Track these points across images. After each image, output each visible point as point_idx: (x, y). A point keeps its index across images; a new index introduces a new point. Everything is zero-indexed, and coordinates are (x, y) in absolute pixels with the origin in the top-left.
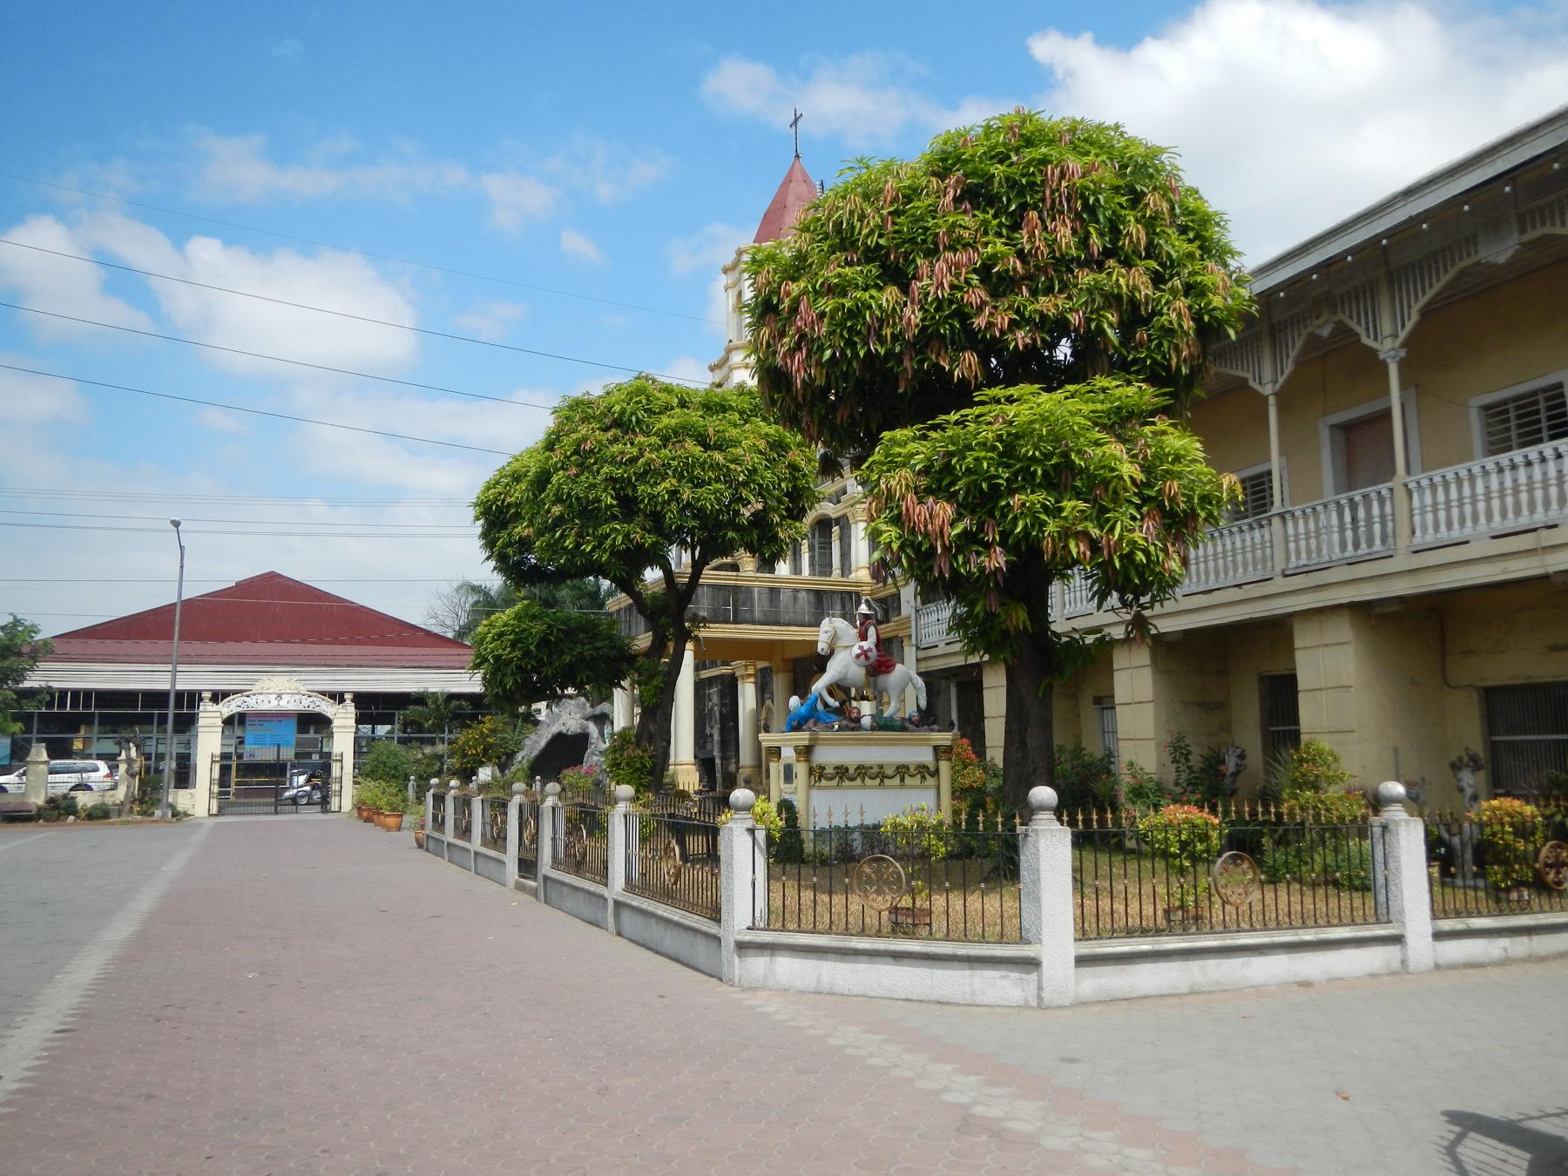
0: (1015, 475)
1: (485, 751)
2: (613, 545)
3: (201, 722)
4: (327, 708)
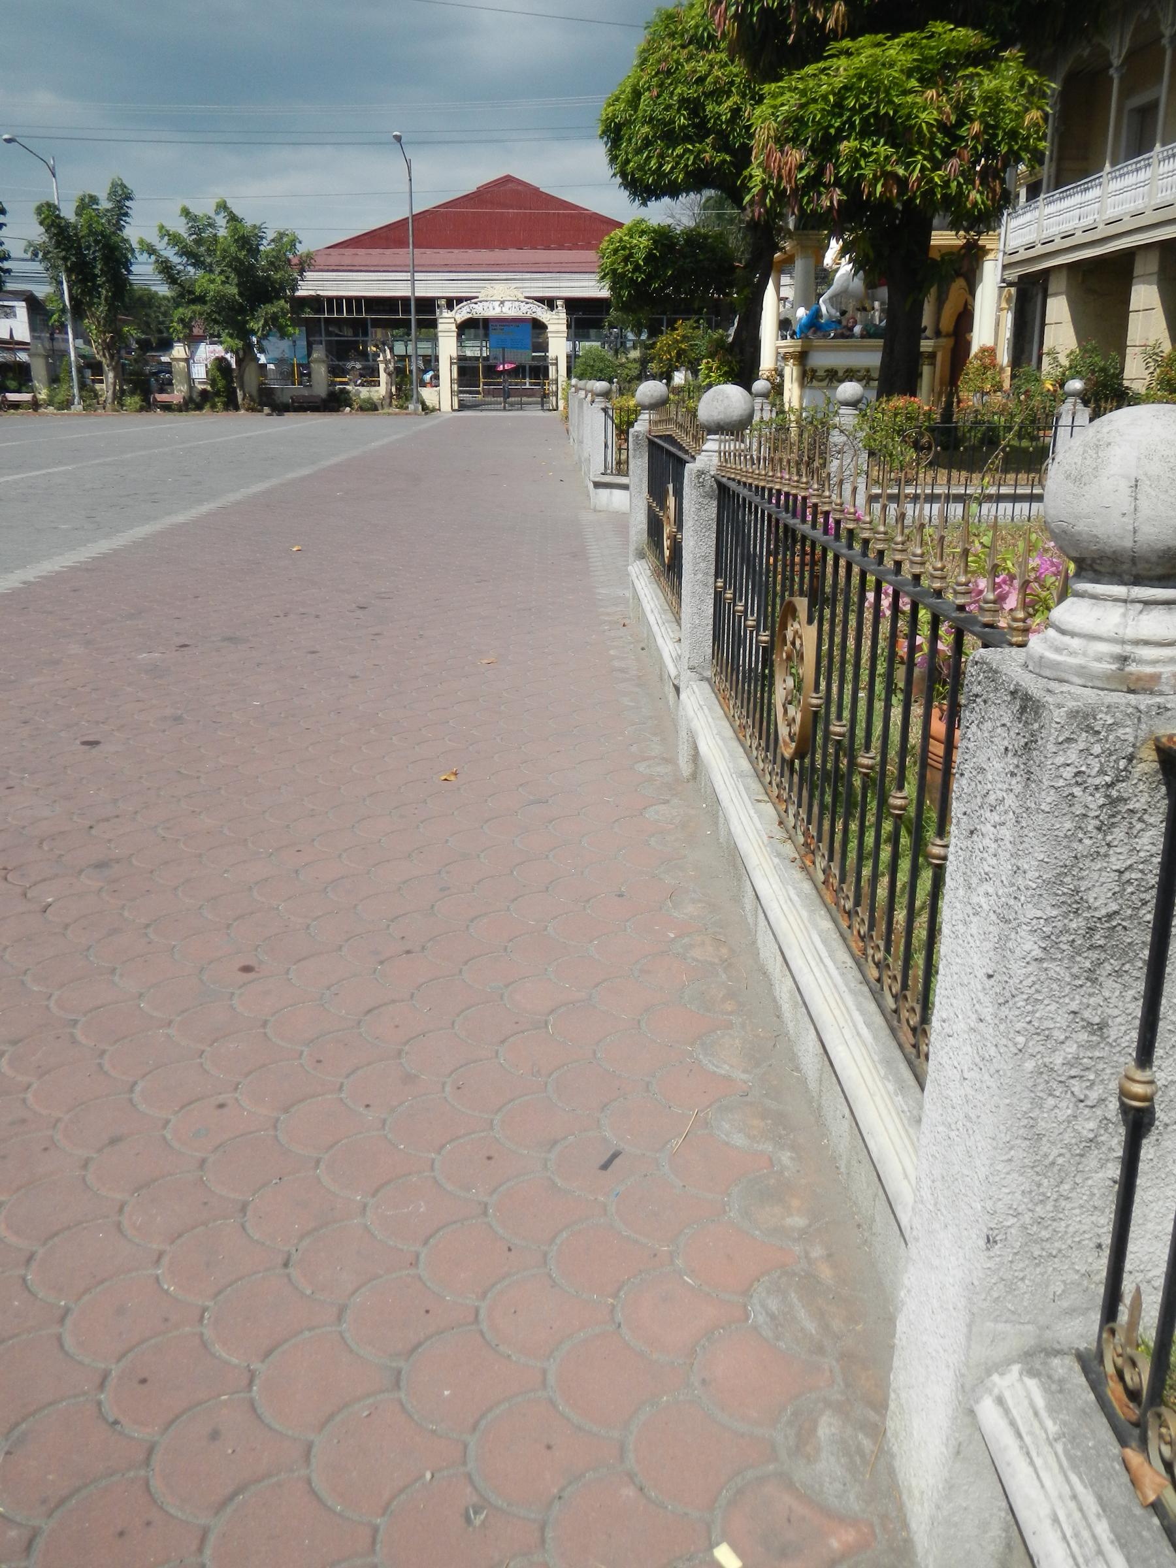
0: (844, 124)
1: (679, 355)
2: (686, 166)
3: (440, 327)
4: (543, 314)
